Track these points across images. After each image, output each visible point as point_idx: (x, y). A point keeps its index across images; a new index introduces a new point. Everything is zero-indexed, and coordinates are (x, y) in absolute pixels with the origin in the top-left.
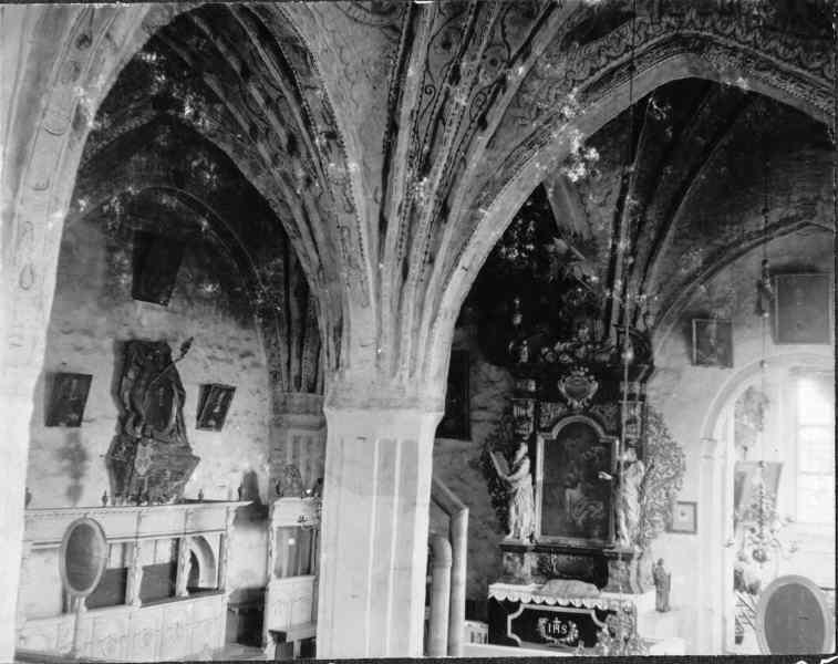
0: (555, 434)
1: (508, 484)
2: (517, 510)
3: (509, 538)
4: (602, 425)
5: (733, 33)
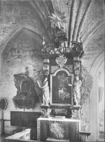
0: (55, 74)
1: (42, 89)
2: (45, 96)
3: (43, 104)
4: (69, 71)
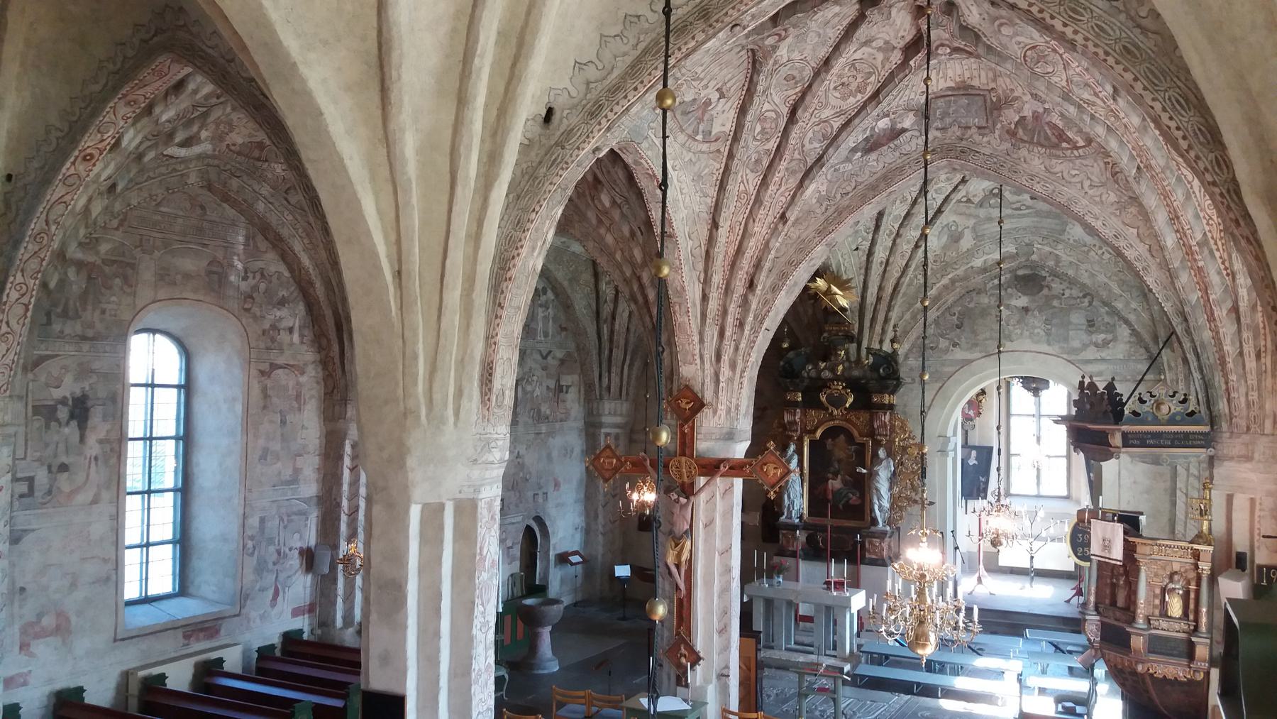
0: (818, 434)
5: (989, 143)
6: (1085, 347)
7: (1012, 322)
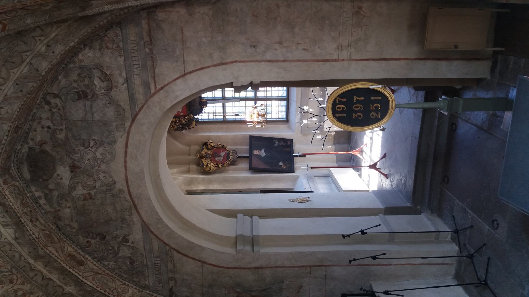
6: (112, 102)
7: (90, 182)
